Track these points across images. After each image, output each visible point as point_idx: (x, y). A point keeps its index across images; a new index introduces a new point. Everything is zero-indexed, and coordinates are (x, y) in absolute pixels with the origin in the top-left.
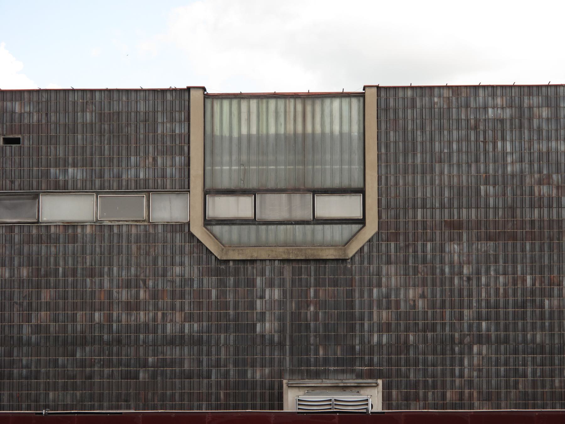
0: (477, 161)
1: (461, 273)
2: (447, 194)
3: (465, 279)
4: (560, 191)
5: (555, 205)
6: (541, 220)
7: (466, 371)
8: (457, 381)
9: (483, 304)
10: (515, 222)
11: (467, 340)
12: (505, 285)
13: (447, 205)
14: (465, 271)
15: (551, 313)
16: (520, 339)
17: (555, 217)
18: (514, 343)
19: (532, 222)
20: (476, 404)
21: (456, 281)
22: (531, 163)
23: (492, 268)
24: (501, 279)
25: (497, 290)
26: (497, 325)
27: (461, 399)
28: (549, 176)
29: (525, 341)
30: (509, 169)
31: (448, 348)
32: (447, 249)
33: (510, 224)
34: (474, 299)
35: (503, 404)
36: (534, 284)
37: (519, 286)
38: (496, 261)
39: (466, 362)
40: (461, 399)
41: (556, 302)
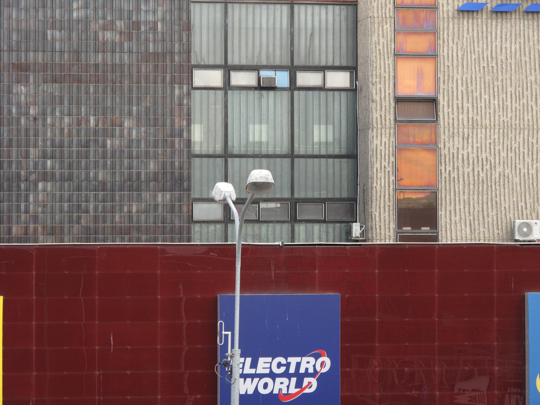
0: (44, 7)
1: (27, 114)
2: (14, 37)
3: (31, 119)
4: (123, 37)
5: (118, 50)
6: (105, 64)
7: (31, 207)
8: (23, 216)
9: (49, 143)
10: (80, 66)
11: (33, 177)
12: (69, 125)
13: (14, 49)
14: (32, 112)
15: (113, 152)
16: (83, 176)
17: (118, 62)
18: (162, 181)
19: (96, 66)
20: (41, 237)
21: (23, 121)
22: (96, 9)
23: (57, 109)
24: (66, 120)
25: (62, 130)
26: (62, 163)
27: (26, 233)
28: (113, 22)
29: (87, 179)
30: (75, 14)
31: (14, 184)
32: (14, 91)
33: (75, 68)
34: (40, 139)
35: (66, 238)
36: (97, 125)
37: (82, 127)
38: (61, 103)
39: (31, 199)
40: (26, 233)
41: (117, 142)
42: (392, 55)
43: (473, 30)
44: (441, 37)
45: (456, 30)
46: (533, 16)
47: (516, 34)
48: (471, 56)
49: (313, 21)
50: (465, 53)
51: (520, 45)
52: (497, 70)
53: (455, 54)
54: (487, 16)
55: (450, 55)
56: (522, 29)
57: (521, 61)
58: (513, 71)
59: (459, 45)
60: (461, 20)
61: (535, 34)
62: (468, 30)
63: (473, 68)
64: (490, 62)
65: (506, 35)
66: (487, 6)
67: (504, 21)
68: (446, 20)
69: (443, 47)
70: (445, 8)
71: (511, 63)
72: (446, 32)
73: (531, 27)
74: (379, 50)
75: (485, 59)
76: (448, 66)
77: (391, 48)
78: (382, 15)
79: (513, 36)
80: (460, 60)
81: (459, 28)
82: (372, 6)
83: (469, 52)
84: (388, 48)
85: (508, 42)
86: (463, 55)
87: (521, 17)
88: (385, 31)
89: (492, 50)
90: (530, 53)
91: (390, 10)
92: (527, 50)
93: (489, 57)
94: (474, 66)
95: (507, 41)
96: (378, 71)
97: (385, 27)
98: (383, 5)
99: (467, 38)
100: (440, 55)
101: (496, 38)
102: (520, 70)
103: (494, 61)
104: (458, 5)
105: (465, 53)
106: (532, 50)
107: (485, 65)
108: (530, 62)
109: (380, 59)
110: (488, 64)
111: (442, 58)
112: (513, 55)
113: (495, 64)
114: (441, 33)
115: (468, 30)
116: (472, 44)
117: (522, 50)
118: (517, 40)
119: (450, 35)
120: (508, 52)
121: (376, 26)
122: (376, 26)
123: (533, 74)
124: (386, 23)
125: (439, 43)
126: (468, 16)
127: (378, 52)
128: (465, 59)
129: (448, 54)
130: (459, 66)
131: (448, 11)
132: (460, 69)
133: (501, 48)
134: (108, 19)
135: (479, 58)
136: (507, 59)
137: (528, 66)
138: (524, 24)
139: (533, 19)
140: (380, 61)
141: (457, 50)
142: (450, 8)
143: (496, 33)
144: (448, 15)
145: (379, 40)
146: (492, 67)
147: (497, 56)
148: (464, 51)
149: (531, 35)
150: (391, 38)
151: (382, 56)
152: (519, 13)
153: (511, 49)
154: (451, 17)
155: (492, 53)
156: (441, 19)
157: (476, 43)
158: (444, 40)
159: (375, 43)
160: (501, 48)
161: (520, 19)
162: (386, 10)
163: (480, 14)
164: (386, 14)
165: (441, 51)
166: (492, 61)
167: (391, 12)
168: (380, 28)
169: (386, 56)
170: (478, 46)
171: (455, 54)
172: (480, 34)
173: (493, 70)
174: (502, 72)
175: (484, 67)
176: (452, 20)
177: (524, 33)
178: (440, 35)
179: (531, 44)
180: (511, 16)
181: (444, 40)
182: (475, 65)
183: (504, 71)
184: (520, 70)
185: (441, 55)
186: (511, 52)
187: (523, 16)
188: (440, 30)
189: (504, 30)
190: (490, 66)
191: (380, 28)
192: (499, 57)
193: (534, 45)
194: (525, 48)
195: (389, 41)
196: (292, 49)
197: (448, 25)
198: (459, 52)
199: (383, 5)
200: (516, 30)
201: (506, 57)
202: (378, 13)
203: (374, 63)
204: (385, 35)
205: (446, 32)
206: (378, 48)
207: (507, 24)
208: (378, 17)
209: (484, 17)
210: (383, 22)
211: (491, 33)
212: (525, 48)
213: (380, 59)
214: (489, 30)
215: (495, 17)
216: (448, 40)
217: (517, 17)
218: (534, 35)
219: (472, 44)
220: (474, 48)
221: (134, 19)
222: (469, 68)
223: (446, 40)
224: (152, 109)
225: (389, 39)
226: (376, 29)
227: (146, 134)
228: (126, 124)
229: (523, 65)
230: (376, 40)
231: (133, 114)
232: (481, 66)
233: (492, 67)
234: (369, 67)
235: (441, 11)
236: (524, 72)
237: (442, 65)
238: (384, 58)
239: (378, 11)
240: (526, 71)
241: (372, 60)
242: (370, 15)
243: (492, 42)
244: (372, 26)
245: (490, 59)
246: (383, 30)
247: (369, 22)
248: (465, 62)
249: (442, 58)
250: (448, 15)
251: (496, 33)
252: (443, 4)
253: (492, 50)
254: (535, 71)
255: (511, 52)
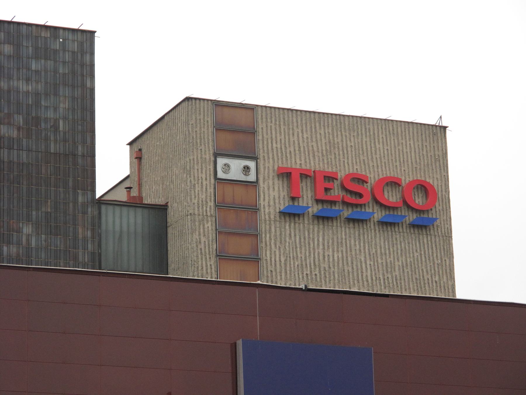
4: (21, 133)
5: (15, 147)
17: (15, 160)
42: (214, 256)
43: (295, 235)
44: (264, 240)
45: (278, 234)
46: (354, 225)
47: (338, 242)
48: (294, 263)
49: (121, 223)
50: (288, 258)
51: (342, 254)
52: (321, 278)
53: (278, 259)
54: (309, 221)
55: (273, 259)
56: (344, 237)
57: (344, 270)
58: (336, 281)
59: (282, 250)
60: (283, 223)
61: (357, 243)
62: (290, 235)
63: (297, 275)
64: (313, 269)
65: (328, 243)
66: (308, 211)
67: (326, 228)
68: (268, 222)
69: (266, 251)
70: (267, 210)
71: (334, 272)
72: (268, 235)
73: (352, 236)
74: (201, 249)
75: (308, 266)
76: (271, 271)
77: (212, 248)
78: (203, 213)
79: (335, 244)
80: (283, 265)
81: (281, 231)
82: (193, 202)
83: (292, 258)
84: (209, 247)
85: (331, 250)
86: (286, 260)
87: (342, 225)
88: (206, 230)
89: (314, 257)
90: (352, 263)
91: (210, 208)
92: (349, 259)
93: (312, 264)
94: (297, 273)
95: (329, 249)
96: (200, 272)
97: (206, 226)
98: (204, 203)
99: (289, 243)
100: (263, 259)
101: (318, 244)
102: (343, 280)
103: (317, 269)
104: (280, 208)
105: (288, 258)
106: (354, 259)
107: (309, 272)
108: (353, 272)
109: (202, 259)
110: (311, 272)
111: (265, 262)
112: (336, 264)
113: (318, 272)
114: (264, 235)
115: (290, 235)
116: (294, 250)
117: (345, 259)
118: (339, 248)
119: (273, 238)
120: (331, 260)
121: (197, 223)
122: (197, 223)
123: (356, 285)
124: (207, 222)
125: (262, 247)
126: (290, 220)
127: (199, 251)
128: (288, 265)
129: (271, 258)
130: (282, 272)
131: (269, 213)
132: (283, 274)
133: (324, 256)
134: (5, 112)
135: (302, 265)
136: (330, 268)
137: (351, 276)
138: (345, 232)
139: (354, 228)
140: (202, 262)
141: (280, 255)
142: (272, 211)
143: (318, 240)
144: (270, 217)
145: (200, 239)
146: (316, 275)
147: (319, 264)
148: (287, 257)
149: (353, 243)
150: (212, 237)
151: (203, 256)
152: (340, 221)
153: (333, 257)
154: (273, 220)
155: (314, 260)
156: (263, 221)
157: (298, 249)
158: (266, 244)
159: (196, 242)
160: (324, 256)
161: (341, 227)
162: (206, 207)
163: (301, 218)
164: (206, 213)
165: (264, 255)
166: (315, 269)
167: (212, 211)
168: (202, 226)
169: (208, 256)
170: (301, 252)
171: (278, 259)
172: (302, 240)
173: (316, 278)
174: (325, 281)
175: (307, 274)
176: (274, 223)
177: (346, 242)
178: (262, 238)
179: (353, 253)
180: (333, 223)
181: (266, 244)
182: (298, 272)
183: (327, 280)
184: (343, 280)
185: (264, 259)
186: (334, 260)
187: (345, 224)
188: (262, 233)
189: (326, 237)
190: (314, 273)
191: (202, 226)
192: (322, 265)
193: (356, 255)
194: (347, 257)
195: (211, 240)
196: (100, 251)
197: (270, 228)
198: (282, 257)
199: (204, 203)
200: (337, 238)
201: (329, 265)
202: (198, 210)
203: (195, 263)
204: (206, 234)
205: (268, 235)
206: (199, 247)
207: (328, 231)
208: (199, 215)
209: (306, 222)
210: (203, 220)
211: (313, 239)
212: (347, 257)
213: (202, 259)
214: (311, 236)
215: (317, 223)
216: (270, 243)
217: (339, 225)
218: (355, 245)
219: (294, 250)
220: (297, 254)
221: (34, 115)
222: (293, 275)
223: (268, 243)
224: (53, 214)
225: (210, 238)
226: (198, 227)
227: (46, 243)
228: (25, 230)
229: (347, 275)
230: (198, 238)
231: (33, 219)
232: (305, 273)
233: (316, 275)
234: (190, 267)
235: (263, 213)
236: (347, 283)
237: (265, 269)
238: (206, 258)
239: (198, 208)
240: (349, 281)
241: (193, 260)
242: (191, 211)
243: (314, 249)
244: (193, 224)
245: (313, 267)
246: (204, 228)
247: (189, 220)
248: (288, 269)
249: (265, 262)
250: (270, 217)
251: (318, 240)
252: (264, 205)
253: (314, 257)
254: (359, 282)
255: (334, 260)
